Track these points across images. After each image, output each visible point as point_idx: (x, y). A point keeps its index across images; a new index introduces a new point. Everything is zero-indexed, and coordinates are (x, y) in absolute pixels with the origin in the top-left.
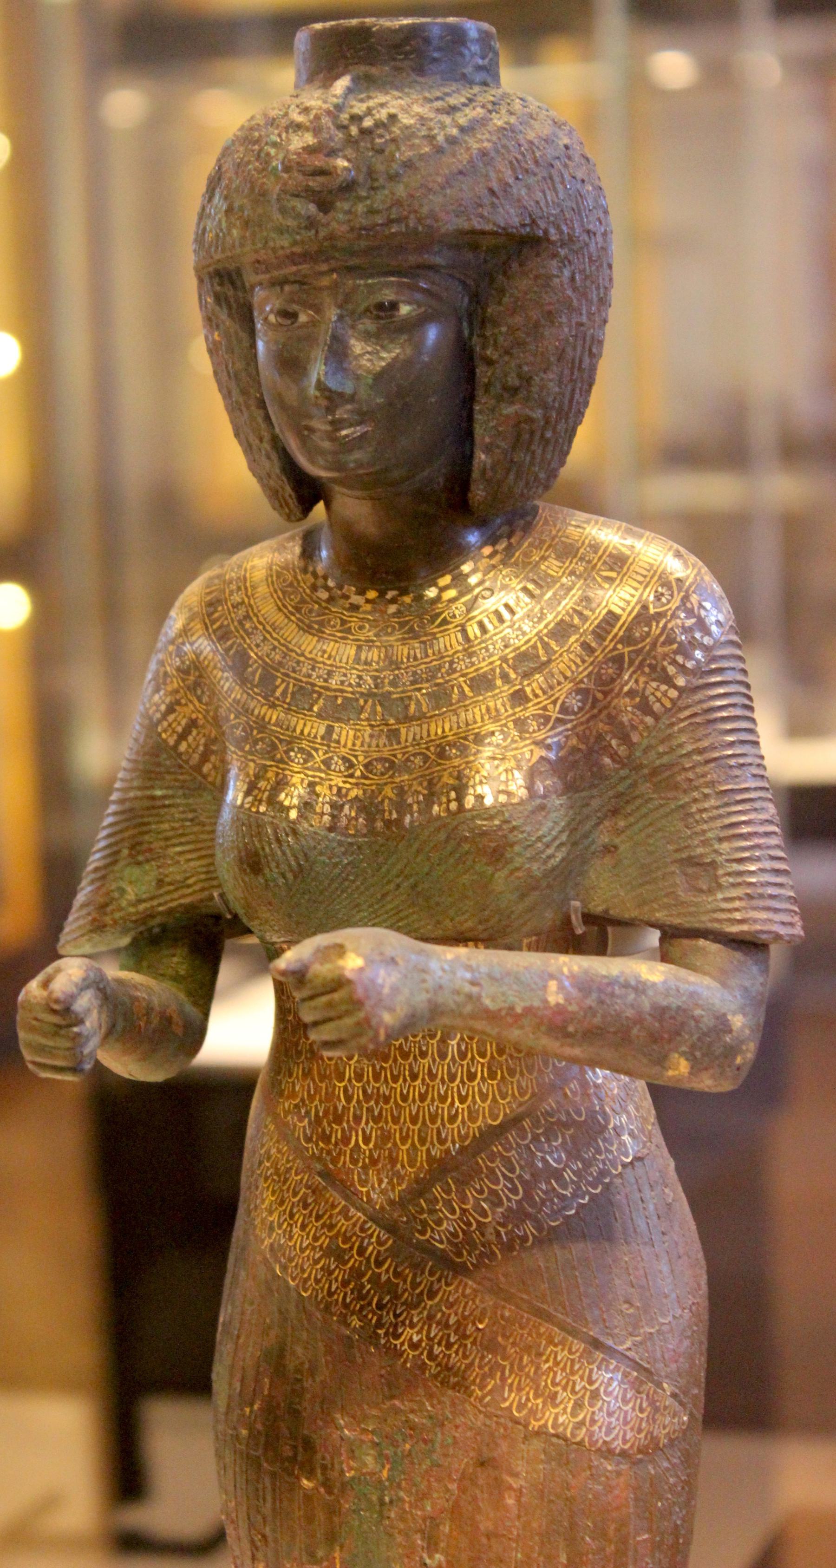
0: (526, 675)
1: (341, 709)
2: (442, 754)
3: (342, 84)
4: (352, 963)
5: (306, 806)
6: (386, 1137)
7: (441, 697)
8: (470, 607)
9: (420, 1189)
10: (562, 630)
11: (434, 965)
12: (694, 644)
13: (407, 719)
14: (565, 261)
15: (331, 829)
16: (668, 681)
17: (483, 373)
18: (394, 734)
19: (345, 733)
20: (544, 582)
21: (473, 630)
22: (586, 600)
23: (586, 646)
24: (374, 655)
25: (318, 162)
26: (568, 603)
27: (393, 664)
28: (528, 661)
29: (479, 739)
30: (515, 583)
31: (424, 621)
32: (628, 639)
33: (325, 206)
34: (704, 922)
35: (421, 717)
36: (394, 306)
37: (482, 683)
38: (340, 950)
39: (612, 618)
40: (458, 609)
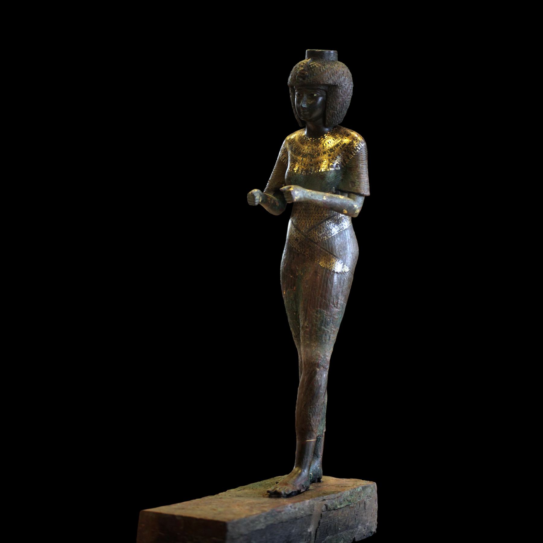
0: (331, 152)
1: (304, 156)
2: (317, 163)
3: (310, 59)
4: (291, 189)
5: (298, 170)
6: (306, 222)
7: (318, 155)
8: (325, 141)
9: (310, 230)
10: (337, 145)
11: (305, 192)
12: (357, 149)
13: (313, 158)
14: (340, 89)
15: (301, 174)
16: (352, 154)
17: (327, 105)
18: (311, 160)
19: (304, 159)
20: (336, 138)
21: (324, 145)
22: (342, 141)
23: (341, 148)
24: (310, 148)
25: (303, 72)
26: (339, 141)
27: (313, 149)
28: (331, 150)
29: (323, 161)
30: (332, 138)
31: (318, 143)
32: (347, 148)
33: (304, 79)
34: (352, 191)
35: (315, 158)
36: (313, 95)
37: (325, 153)
38: (290, 187)
39: (345, 144)
40: (323, 141)
